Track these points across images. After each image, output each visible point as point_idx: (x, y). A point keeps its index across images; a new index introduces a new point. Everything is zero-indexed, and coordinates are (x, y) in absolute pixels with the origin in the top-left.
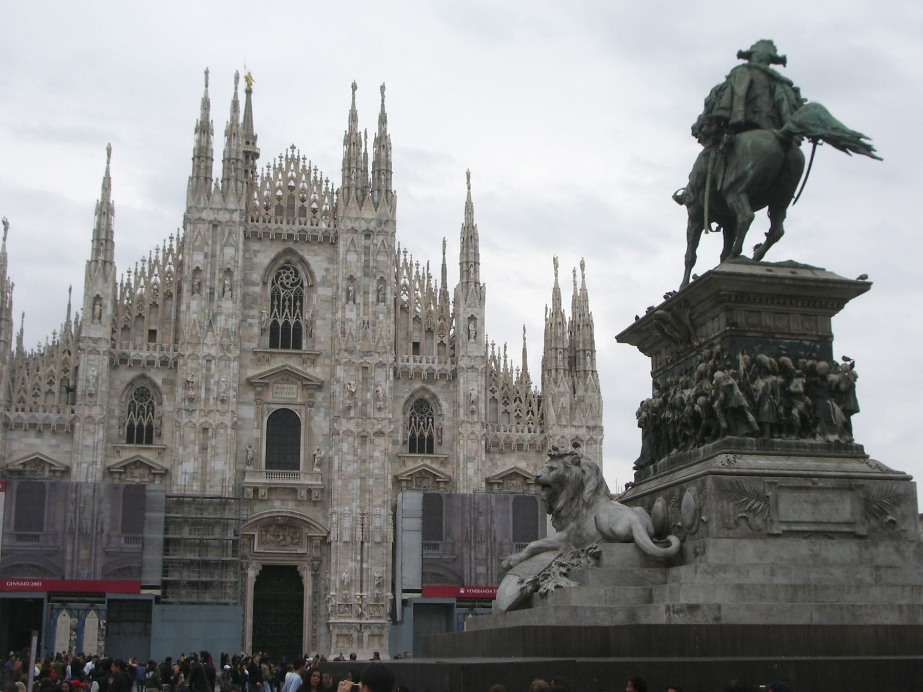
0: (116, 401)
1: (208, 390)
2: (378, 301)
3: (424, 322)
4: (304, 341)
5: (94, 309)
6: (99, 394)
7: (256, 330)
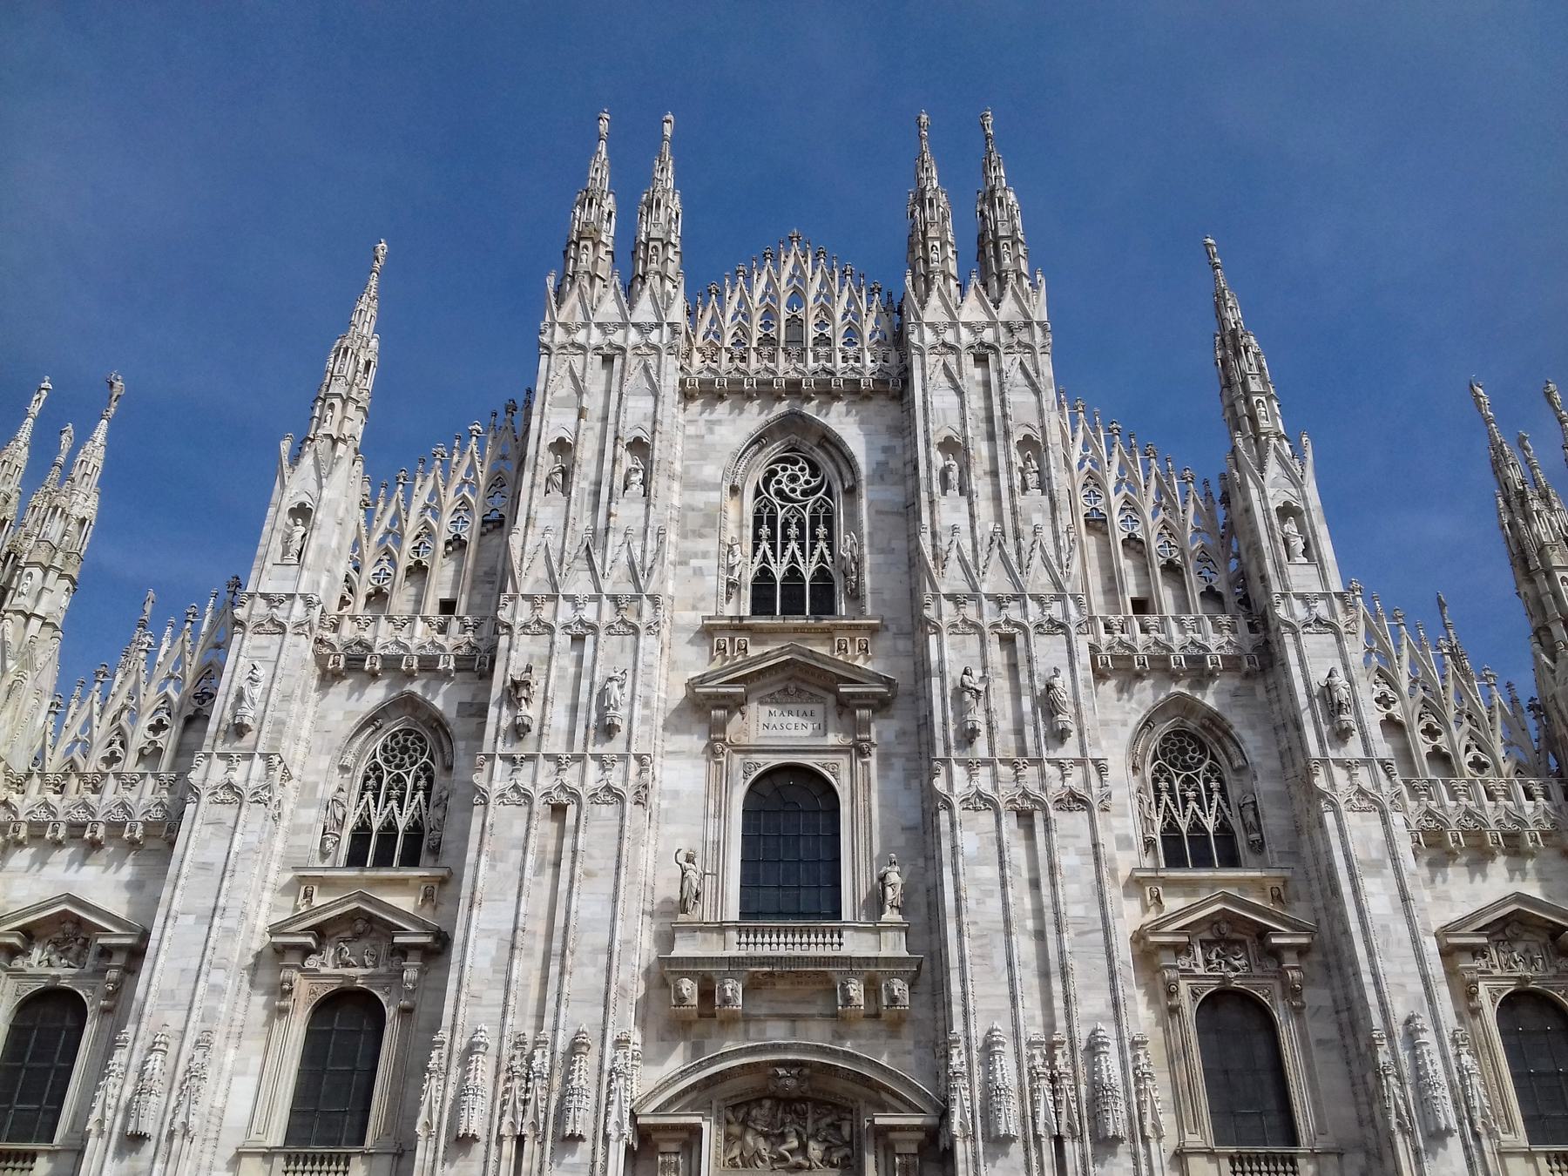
0: (324, 762)
1: (574, 709)
2: (1025, 488)
3: (1154, 545)
4: (842, 607)
5: (288, 539)
6: (266, 728)
7: (713, 582)
